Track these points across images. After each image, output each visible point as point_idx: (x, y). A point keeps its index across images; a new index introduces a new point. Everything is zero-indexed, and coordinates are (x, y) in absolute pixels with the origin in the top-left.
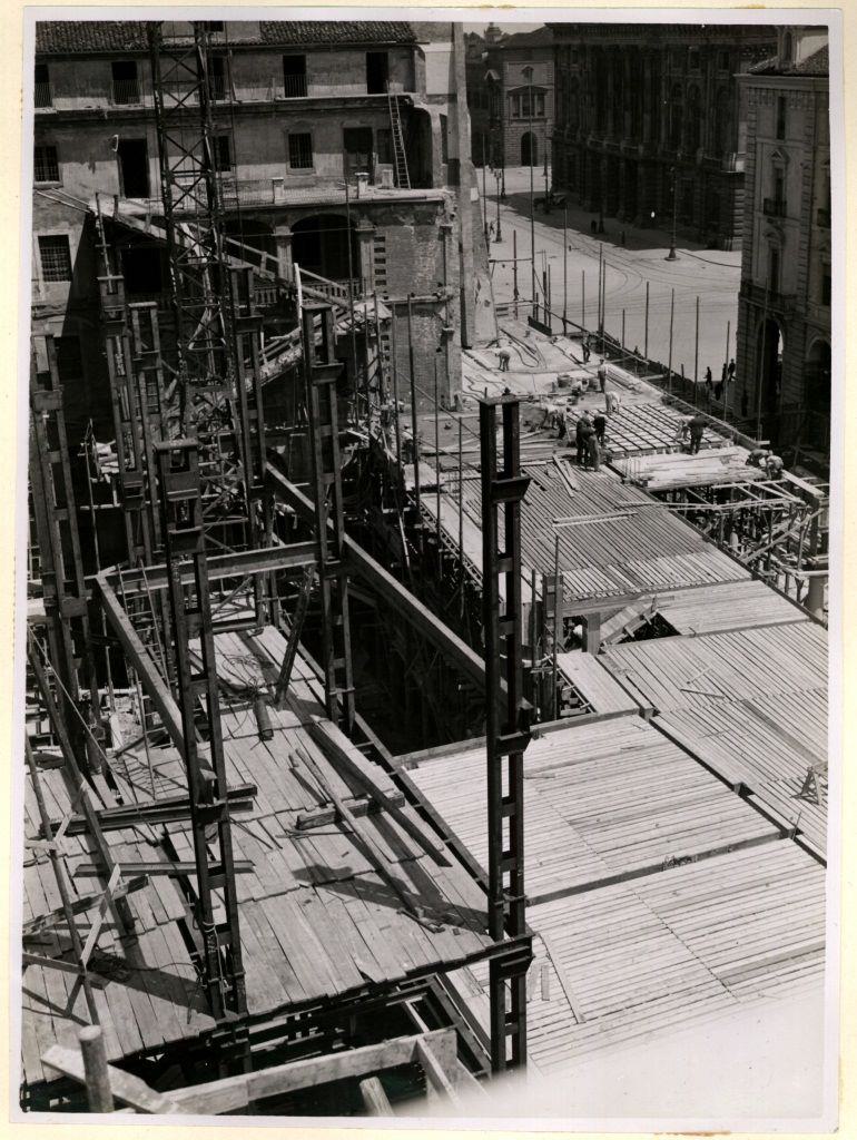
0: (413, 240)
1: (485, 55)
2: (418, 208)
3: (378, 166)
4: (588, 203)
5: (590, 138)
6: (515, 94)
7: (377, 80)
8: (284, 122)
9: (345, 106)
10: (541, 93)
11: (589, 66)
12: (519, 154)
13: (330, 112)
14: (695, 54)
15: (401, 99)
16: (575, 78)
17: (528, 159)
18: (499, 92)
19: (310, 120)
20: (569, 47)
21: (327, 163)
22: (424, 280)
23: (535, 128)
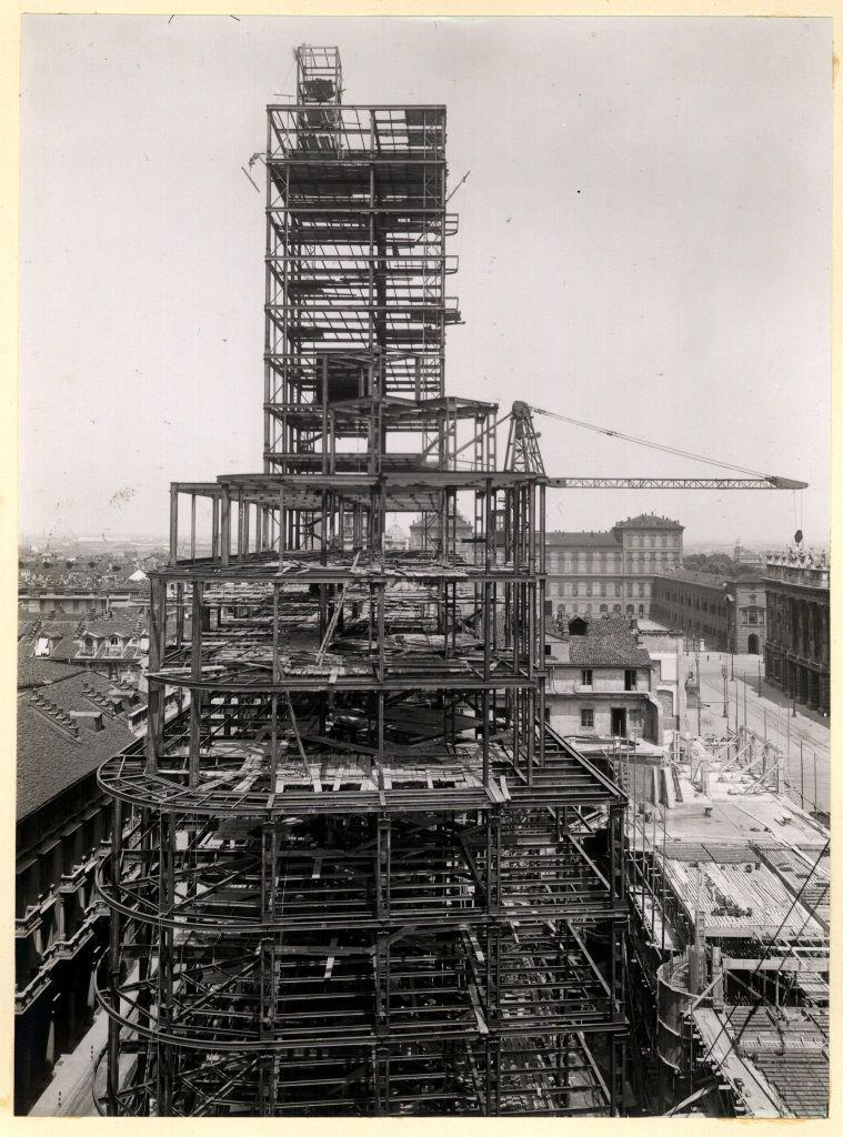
1: (725, 585)
3: (629, 724)
6: (744, 610)
7: (630, 680)
8: (580, 703)
9: (611, 697)
10: (762, 610)
12: (746, 645)
13: (604, 700)
15: (643, 695)
17: (753, 649)
18: (734, 608)
19: (592, 702)
21: (603, 720)
23: (757, 632)
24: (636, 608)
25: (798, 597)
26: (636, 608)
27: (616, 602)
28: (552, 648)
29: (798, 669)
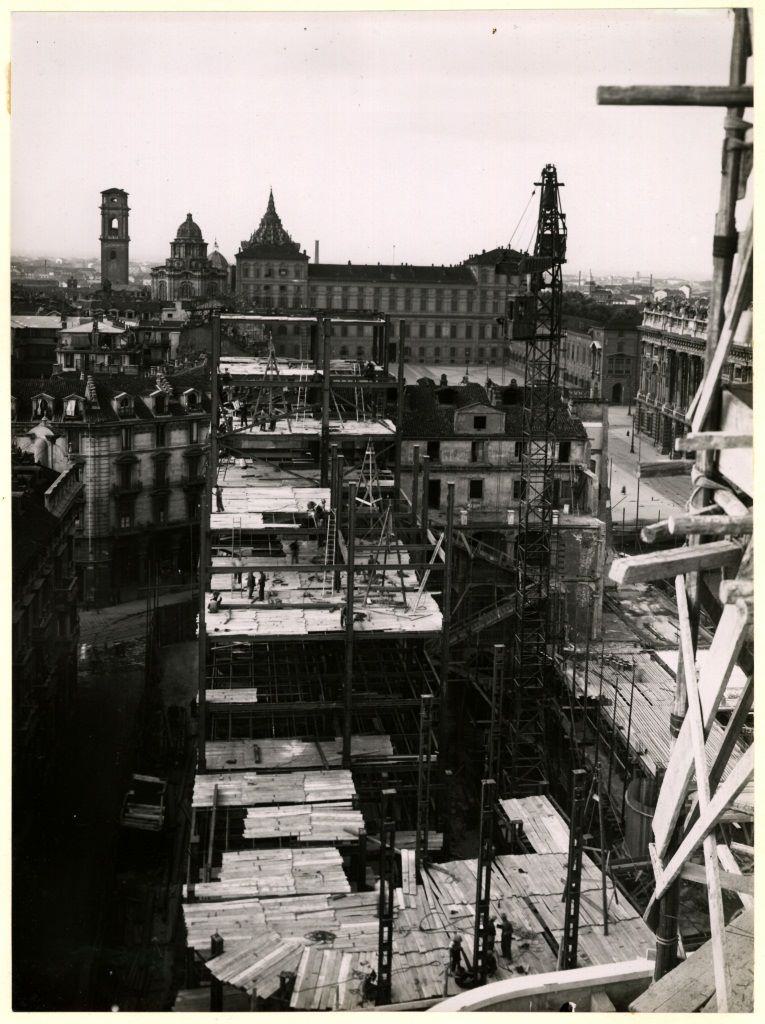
0: (581, 547)
2: (584, 531)
4: (660, 448)
5: (663, 407)
8: (512, 474)
11: (666, 361)
14: (738, 370)
16: (655, 365)
20: (652, 345)
22: (584, 569)
24: (488, 351)
25: (679, 349)
26: (488, 351)
27: (468, 345)
28: (488, 420)
29: (674, 424)
